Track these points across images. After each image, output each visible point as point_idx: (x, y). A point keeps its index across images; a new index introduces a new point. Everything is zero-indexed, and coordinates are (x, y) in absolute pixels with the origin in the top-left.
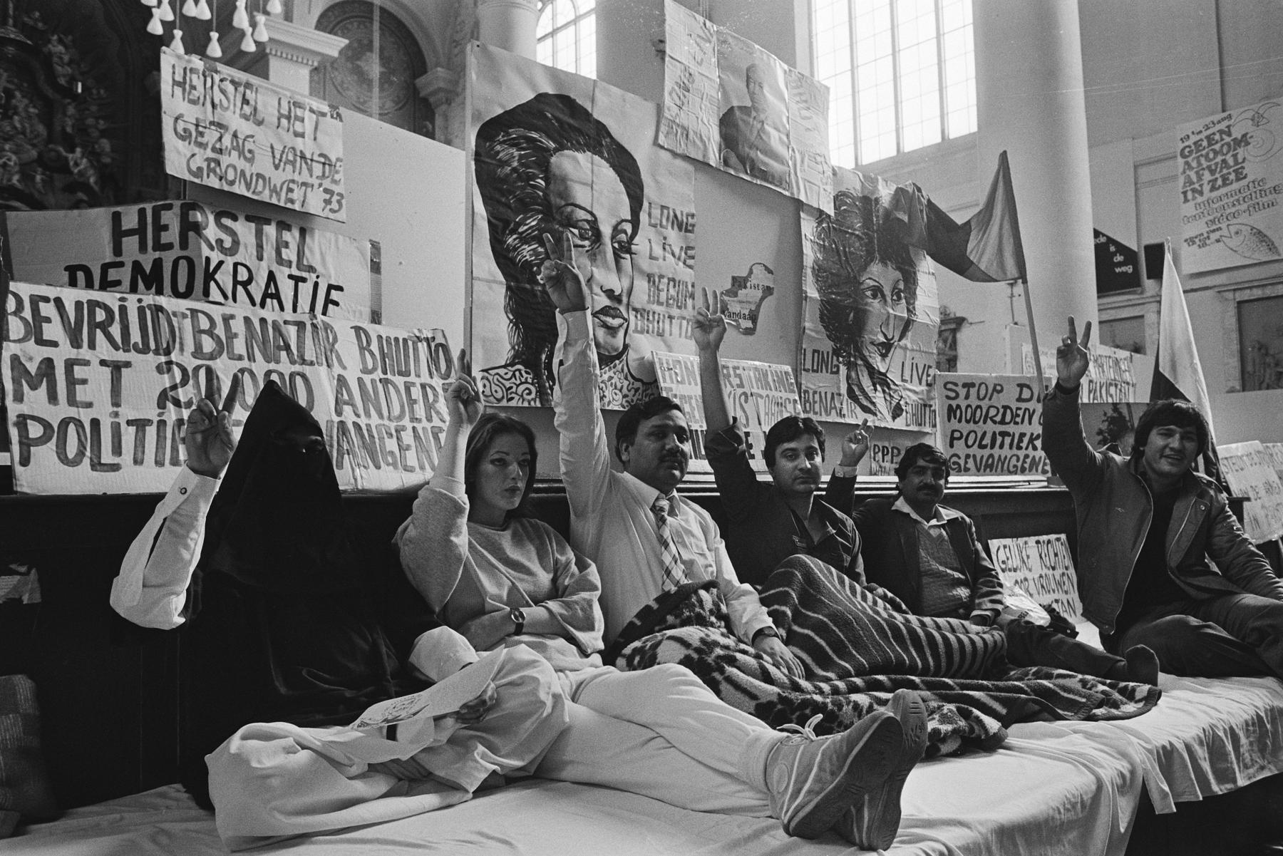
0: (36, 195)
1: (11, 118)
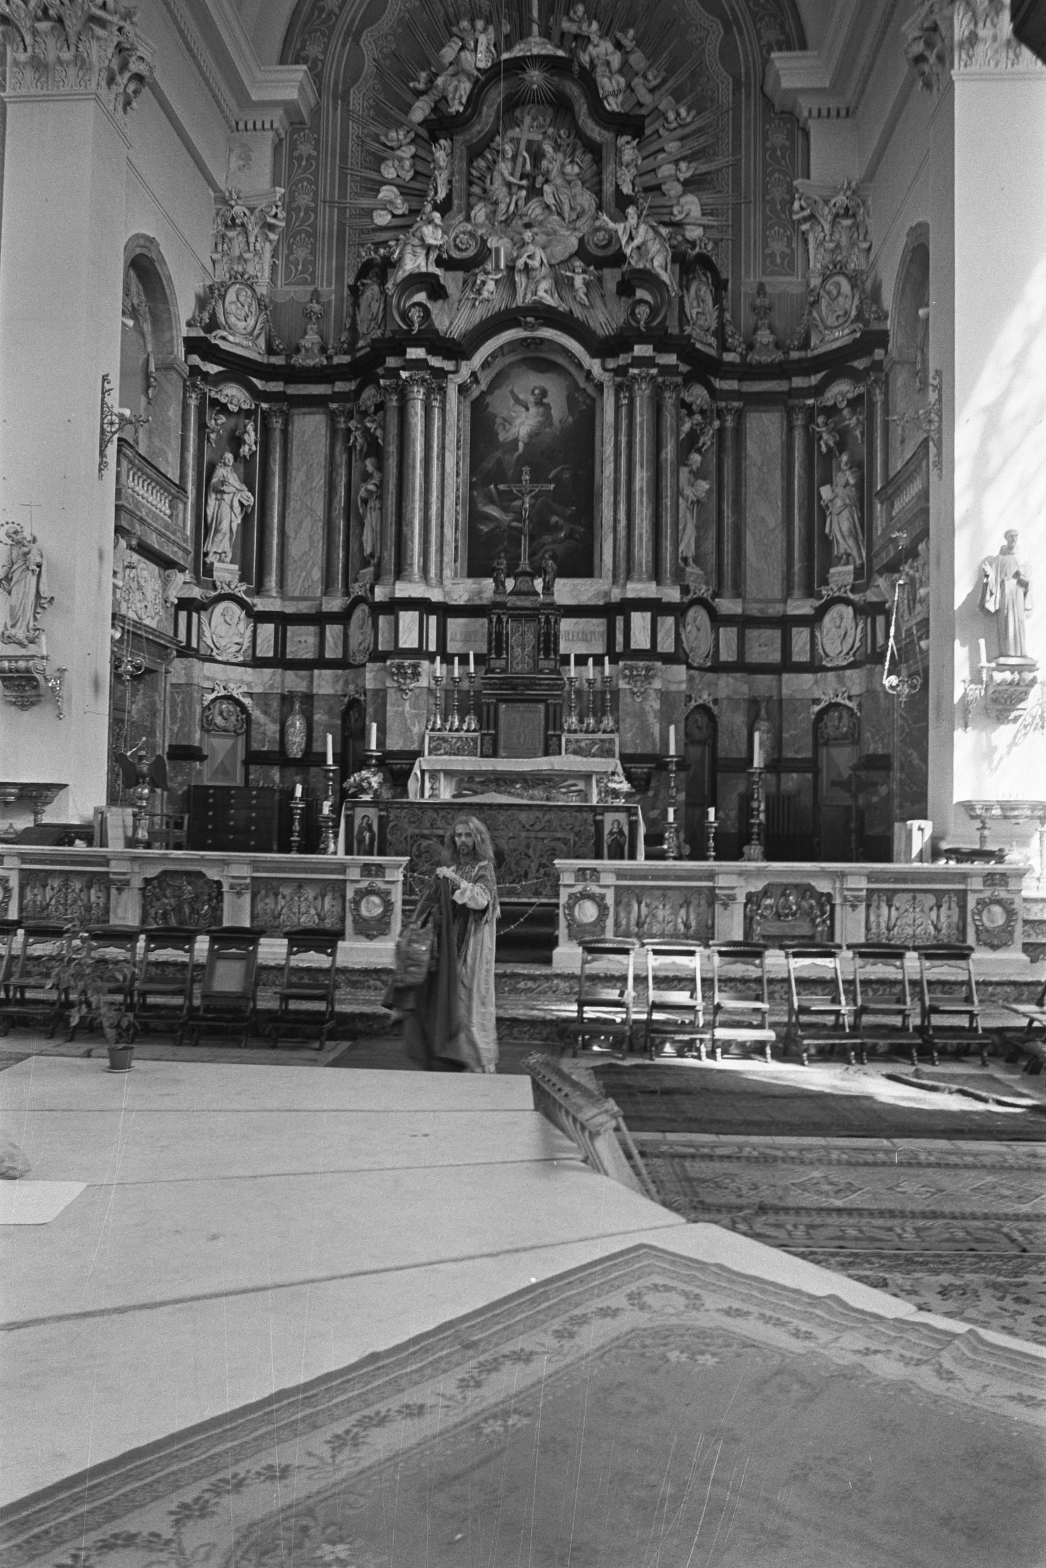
0: (578, 313)
1: (540, 193)
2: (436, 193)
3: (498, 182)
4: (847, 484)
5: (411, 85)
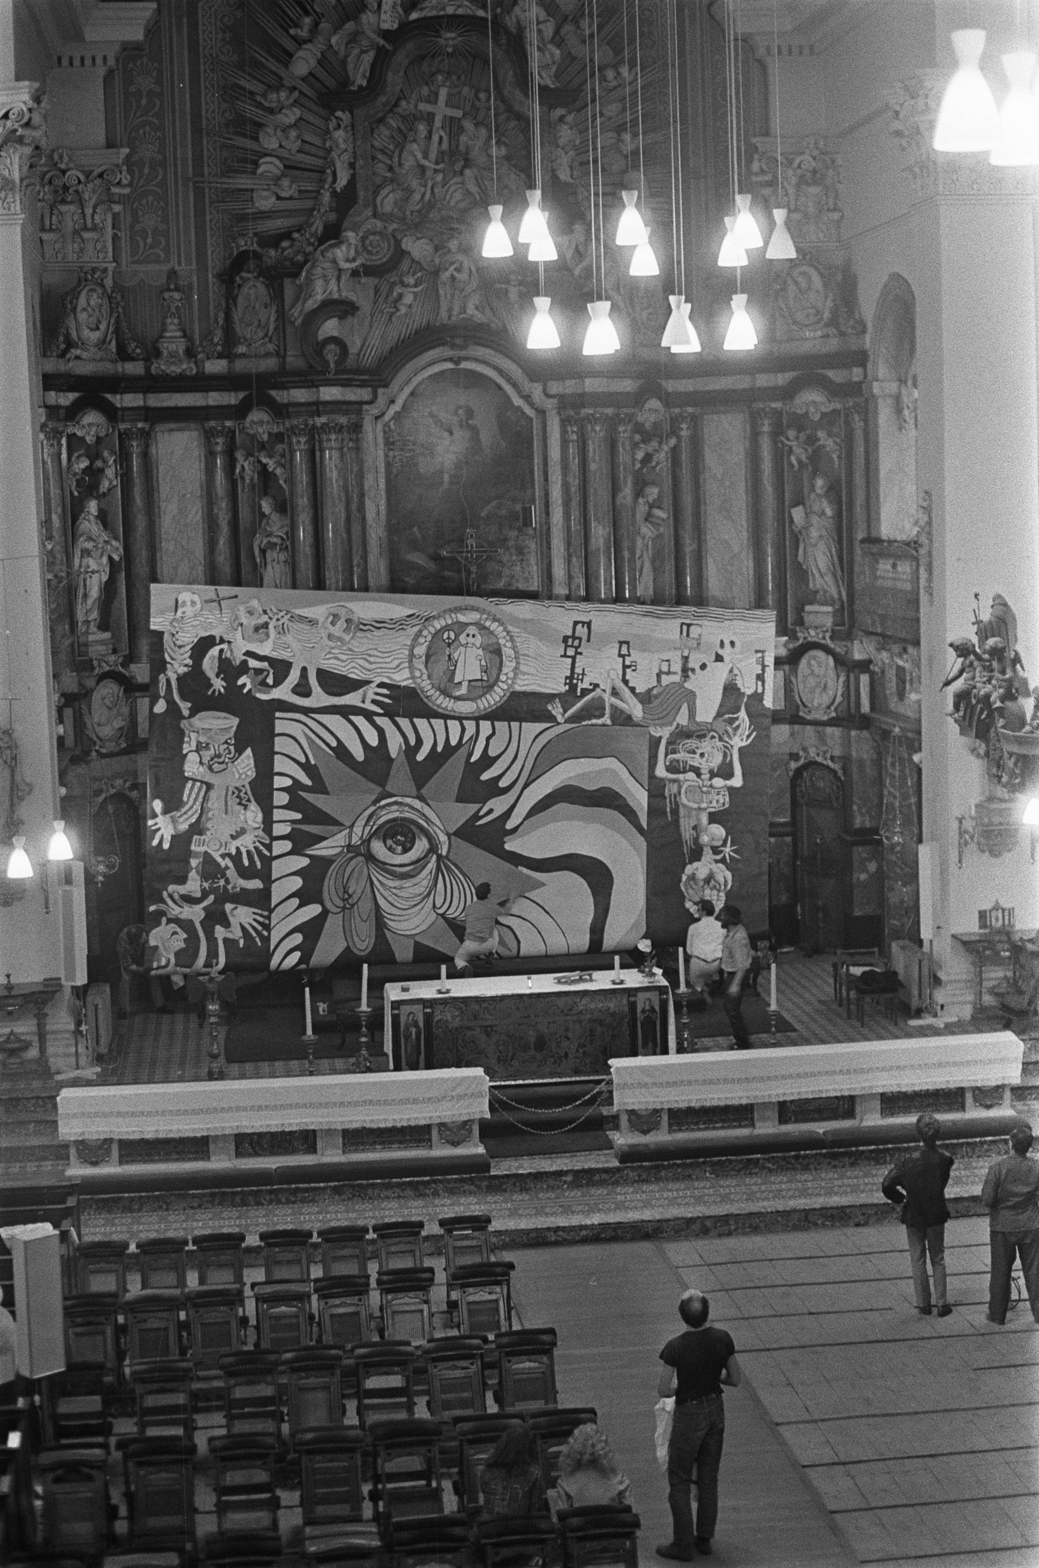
2: (334, 181)
3: (409, 162)
4: (823, 513)
5: (292, 31)
